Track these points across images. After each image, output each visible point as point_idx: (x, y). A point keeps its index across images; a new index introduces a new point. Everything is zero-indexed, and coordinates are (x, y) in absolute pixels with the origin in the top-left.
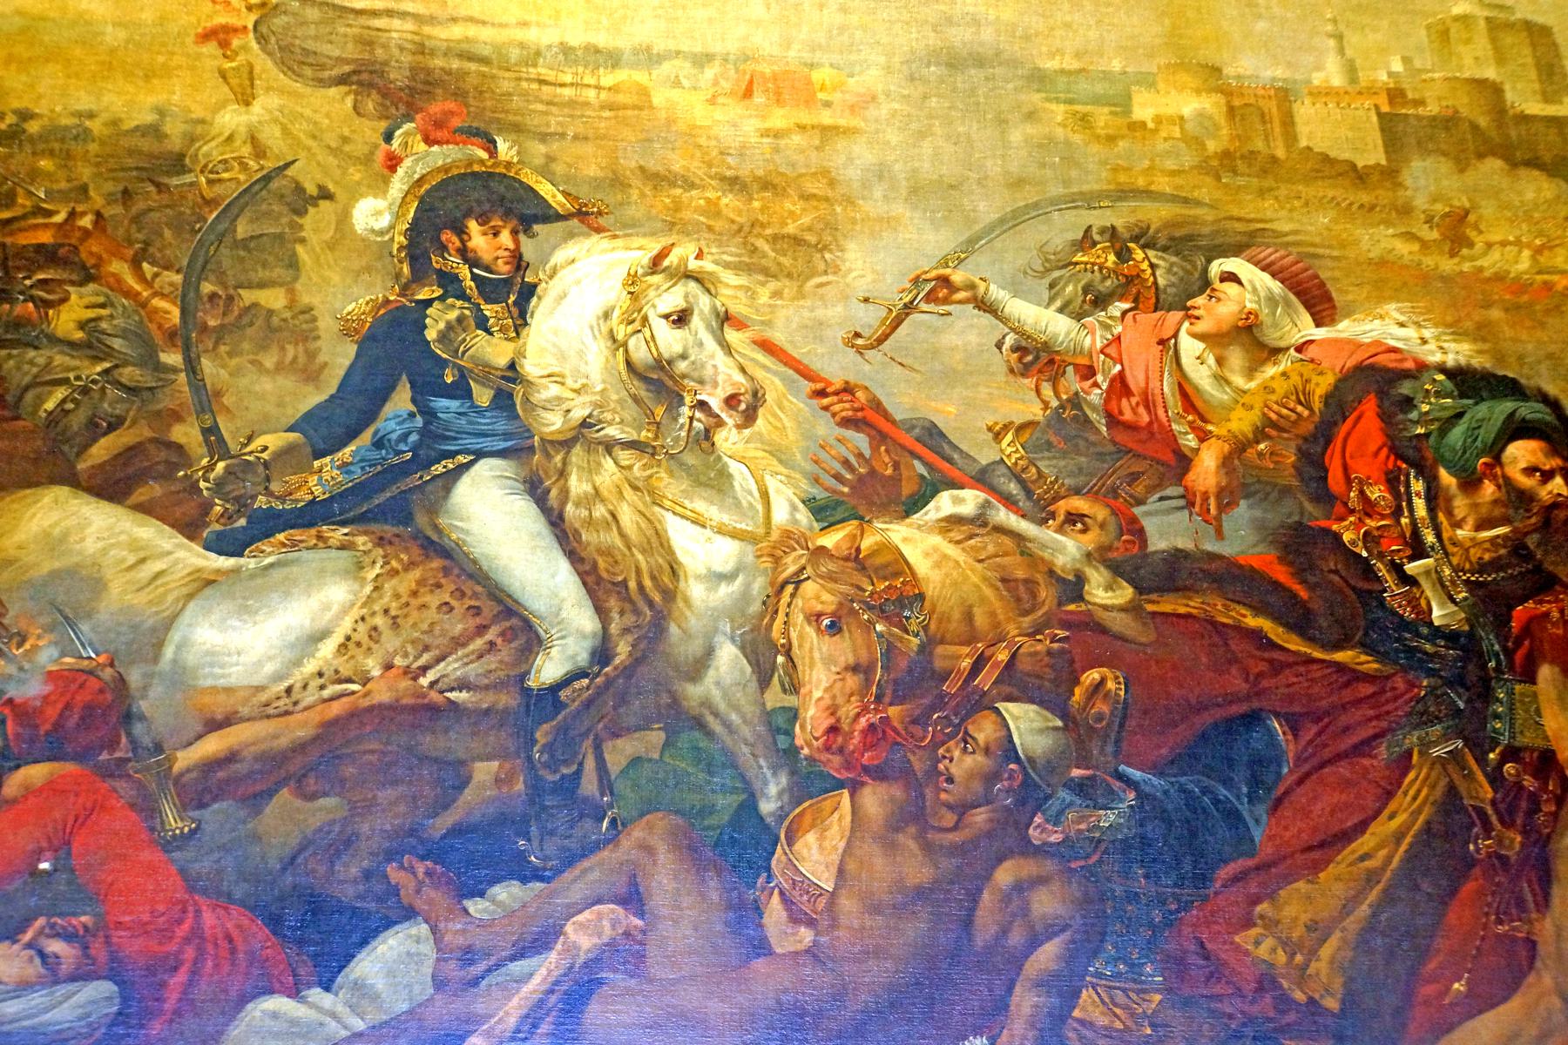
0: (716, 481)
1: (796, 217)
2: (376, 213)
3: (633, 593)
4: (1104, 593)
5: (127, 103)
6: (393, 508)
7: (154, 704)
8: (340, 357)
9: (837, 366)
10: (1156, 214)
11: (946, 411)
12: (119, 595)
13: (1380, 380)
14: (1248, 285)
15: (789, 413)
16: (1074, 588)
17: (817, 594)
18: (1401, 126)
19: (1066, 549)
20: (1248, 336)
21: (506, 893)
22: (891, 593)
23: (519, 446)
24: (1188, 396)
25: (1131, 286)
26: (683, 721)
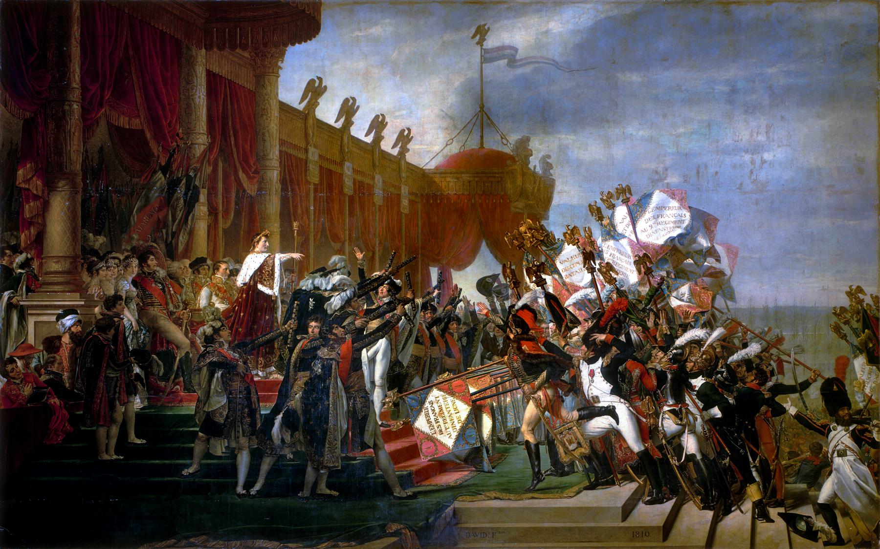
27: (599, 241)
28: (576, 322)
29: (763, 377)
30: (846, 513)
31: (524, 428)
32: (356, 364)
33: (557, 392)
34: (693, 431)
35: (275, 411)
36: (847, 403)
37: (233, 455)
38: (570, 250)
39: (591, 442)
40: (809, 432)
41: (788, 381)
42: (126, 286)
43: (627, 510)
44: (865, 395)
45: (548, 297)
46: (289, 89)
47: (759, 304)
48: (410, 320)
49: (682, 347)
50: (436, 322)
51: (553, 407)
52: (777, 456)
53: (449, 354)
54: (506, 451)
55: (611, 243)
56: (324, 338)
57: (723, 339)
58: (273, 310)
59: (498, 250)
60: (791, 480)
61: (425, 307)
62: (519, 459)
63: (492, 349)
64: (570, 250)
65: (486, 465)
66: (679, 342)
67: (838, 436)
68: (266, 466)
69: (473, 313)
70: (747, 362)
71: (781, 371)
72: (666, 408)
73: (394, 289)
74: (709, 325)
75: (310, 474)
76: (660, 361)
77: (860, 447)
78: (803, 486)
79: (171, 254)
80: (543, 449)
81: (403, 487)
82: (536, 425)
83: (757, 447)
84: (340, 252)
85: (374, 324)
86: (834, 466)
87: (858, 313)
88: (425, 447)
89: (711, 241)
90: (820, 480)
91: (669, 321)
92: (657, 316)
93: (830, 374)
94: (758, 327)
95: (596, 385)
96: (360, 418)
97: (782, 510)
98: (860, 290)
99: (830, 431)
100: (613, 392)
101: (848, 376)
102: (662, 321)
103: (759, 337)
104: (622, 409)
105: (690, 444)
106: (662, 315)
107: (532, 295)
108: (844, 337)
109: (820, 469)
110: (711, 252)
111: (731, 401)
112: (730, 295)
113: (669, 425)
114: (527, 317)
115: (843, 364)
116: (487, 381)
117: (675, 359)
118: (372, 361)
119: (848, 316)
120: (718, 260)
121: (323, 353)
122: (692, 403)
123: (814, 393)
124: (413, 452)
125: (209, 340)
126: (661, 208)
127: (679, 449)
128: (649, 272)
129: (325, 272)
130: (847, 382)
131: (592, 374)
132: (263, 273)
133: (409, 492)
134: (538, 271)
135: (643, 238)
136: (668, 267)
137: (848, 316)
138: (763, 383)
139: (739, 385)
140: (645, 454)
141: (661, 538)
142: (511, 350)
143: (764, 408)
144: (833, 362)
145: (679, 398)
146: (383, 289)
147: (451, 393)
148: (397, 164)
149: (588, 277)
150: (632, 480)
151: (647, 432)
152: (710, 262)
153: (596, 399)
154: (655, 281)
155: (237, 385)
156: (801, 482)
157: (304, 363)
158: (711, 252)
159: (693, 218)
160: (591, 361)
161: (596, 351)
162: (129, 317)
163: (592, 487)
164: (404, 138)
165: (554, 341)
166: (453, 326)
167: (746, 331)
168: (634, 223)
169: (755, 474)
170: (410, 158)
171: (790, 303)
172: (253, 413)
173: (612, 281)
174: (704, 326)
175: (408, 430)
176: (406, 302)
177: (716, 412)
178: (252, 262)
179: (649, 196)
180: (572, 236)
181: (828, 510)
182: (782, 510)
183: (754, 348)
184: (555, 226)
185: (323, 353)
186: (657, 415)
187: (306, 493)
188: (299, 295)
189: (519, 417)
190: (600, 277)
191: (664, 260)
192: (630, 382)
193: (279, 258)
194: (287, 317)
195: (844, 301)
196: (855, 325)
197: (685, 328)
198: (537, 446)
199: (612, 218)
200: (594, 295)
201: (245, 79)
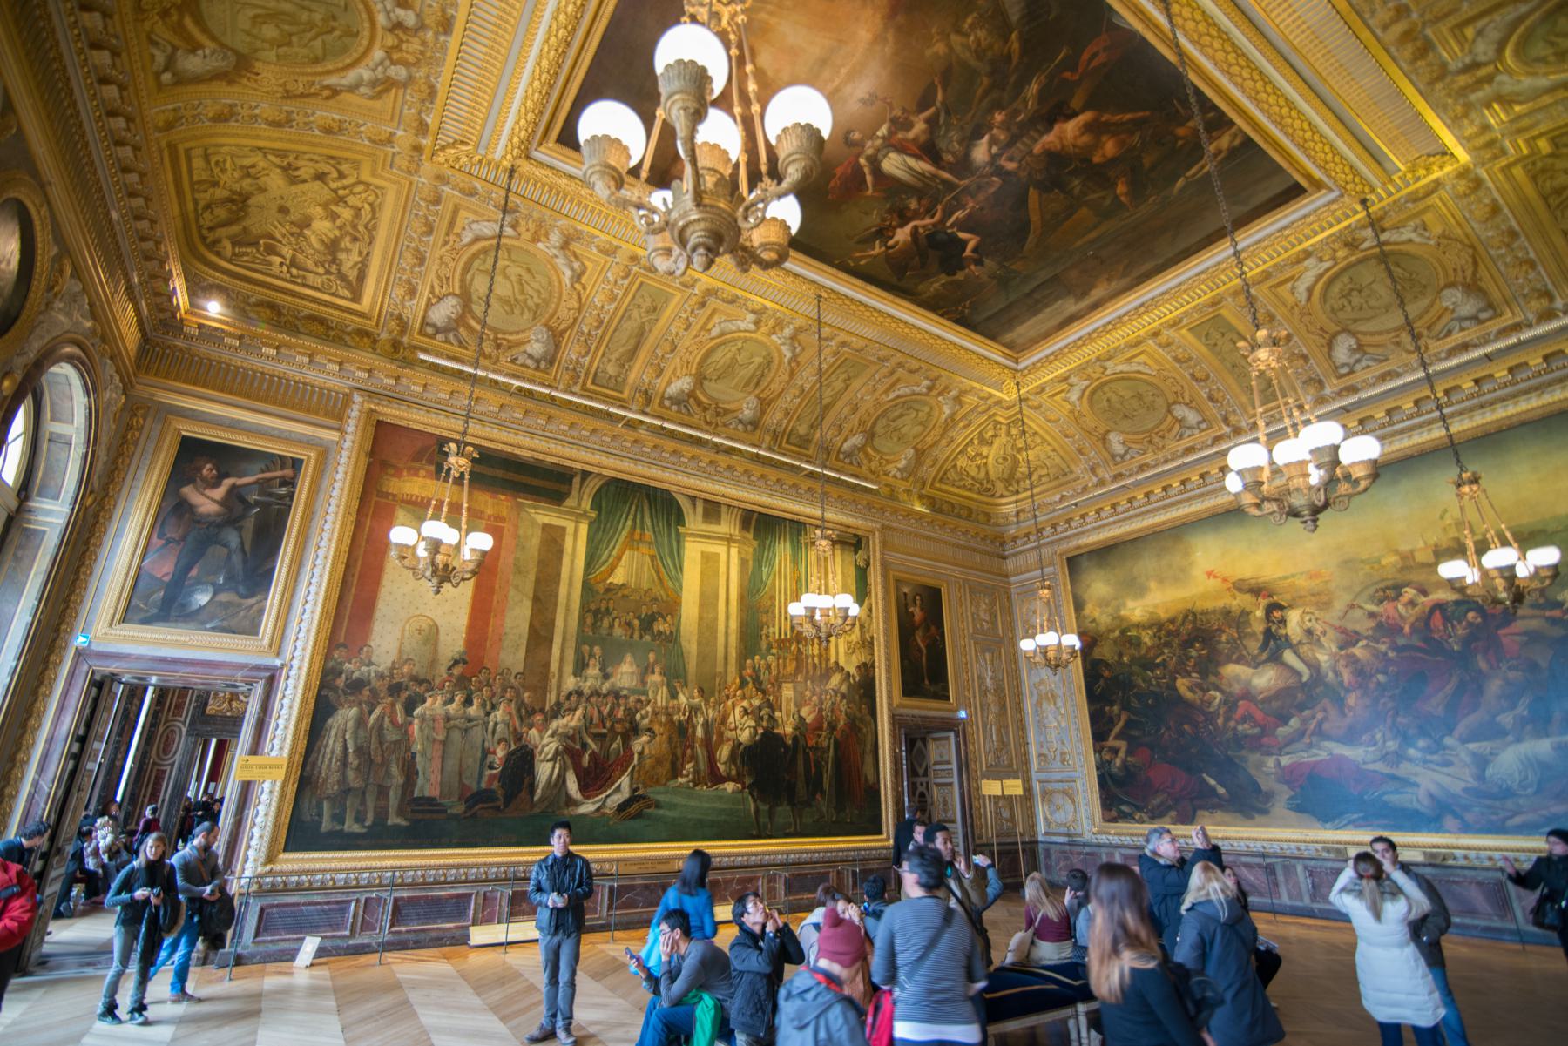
0: (1321, 646)
1: (1325, 598)
2: (1260, 613)
3: (1314, 666)
4: (1391, 654)
5: (1220, 604)
6: (1275, 658)
8: (1261, 637)
9: (1337, 623)
10: (1389, 583)
11: (1358, 627)
13: (1439, 606)
14: (1409, 593)
15: (1331, 633)
16: (1385, 654)
17: (1342, 662)
20: (1412, 603)
21: (1307, 713)
22: (1353, 660)
23: (1290, 646)
24: (1401, 616)
25: (1387, 598)
26: (1326, 685)
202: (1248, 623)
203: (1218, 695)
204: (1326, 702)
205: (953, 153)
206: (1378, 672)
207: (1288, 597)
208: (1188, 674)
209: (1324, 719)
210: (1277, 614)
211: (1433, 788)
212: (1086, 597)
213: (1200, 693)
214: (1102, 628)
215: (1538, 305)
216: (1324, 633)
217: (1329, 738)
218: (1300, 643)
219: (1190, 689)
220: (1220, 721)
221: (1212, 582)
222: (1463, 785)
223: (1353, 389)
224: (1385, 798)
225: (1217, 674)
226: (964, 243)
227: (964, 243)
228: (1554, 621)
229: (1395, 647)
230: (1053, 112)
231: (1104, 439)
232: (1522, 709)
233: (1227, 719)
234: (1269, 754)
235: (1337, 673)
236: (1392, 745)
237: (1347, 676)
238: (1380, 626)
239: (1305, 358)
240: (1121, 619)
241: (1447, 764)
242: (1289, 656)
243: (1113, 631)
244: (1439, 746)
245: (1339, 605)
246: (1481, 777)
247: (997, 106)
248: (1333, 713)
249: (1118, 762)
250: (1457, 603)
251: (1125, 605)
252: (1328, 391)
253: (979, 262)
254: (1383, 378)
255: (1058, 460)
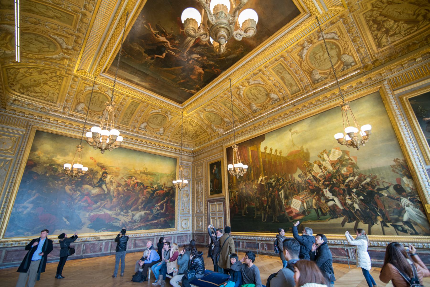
0: (112, 185)
1: (118, 174)
2: (101, 173)
3: (109, 190)
4: (126, 191)
6: (100, 186)
7: (90, 194)
8: (99, 180)
9: (118, 181)
11: (122, 183)
12: (89, 189)
13: (137, 183)
14: (134, 178)
15: (116, 183)
18: (141, 172)
19: (125, 189)
20: (133, 181)
21: (103, 201)
22: (118, 190)
25: (129, 178)
26: (110, 195)
27: (322, 162)
28: (320, 180)
29: (373, 187)
30: (416, 224)
31: (313, 205)
32: (279, 195)
33: (319, 197)
34: (356, 203)
35: (267, 206)
36: (404, 191)
37: (261, 215)
38: (316, 166)
39: (330, 207)
40: (393, 200)
41: (382, 187)
42: (244, 186)
43: (343, 224)
44: (410, 188)
45: (313, 176)
46: (262, 149)
47: (367, 168)
48: (287, 185)
49: (348, 182)
50: (291, 185)
51: (319, 200)
52: (384, 208)
53: (295, 191)
54: (310, 211)
55: (324, 162)
56: (273, 191)
57: (358, 179)
58: (264, 187)
59: (301, 168)
60: (391, 215)
61: (289, 182)
62: (313, 213)
63: (303, 189)
64: (316, 166)
65: (307, 214)
66: (346, 181)
67: (405, 201)
68: (266, 216)
69: (298, 182)
70: (367, 184)
71: (379, 184)
72: (347, 198)
73: (283, 180)
74: (354, 176)
75: (274, 218)
76: (343, 186)
77: (414, 203)
78: (396, 216)
79: (249, 180)
80: (319, 210)
81: (291, 220)
82: (316, 204)
83: (377, 206)
84: (273, 175)
85: (281, 187)
86: (406, 210)
87: (399, 165)
88: (294, 211)
89: (349, 156)
90: (402, 214)
91: (343, 177)
92: (339, 176)
93: (395, 183)
94: (368, 174)
95: (328, 195)
96: (281, 205)
97: (391, 224)
98: (397, 159)
99: (401, 199)
100: (332, 195)
101: (402, 183)
102: (341, 177)
103: (369, 177)
104: (336, 199)
105: (356, 206)
106: (340, 176)
107: (309, 176)
108: (397, 173)
109: (401, 211)
110: (349, 159)
111: (365, 194)
112: (358, 168)
113: (349, 202)
114: (309, 181)
115: (399, 180)
116: (303, 196)
117: (346, 186)
118: (281, 194)
119: (396, 167)
120: (352, 160)
121: (273, 194)
122: (354, 195)
123: (391, 189)
124: (291, 212)
125: (255, 193)
126: (334, 152)
127: (354, 208)
128: (335, 167)
129: (271, 179)
130: (402, 185)
131: (326, 191)
132: (262, 181)
133: (292, 221)
134: (310, 171)
135: (331, 159)
136: (339, 164)
137: (396, 167)
138: (374, 188)
139: (367, 190)
140: (344, 210)
141: (354, 231)
142: (307, 189)
143: (376, 195)
144: (395, 180)
145: (350, 195)
146: (281, 180)
147: (297, 199)
148: (280, 157)
149: (321, 170)
150: (342, 216)
151: (344, 204)
152: (350, 161)
153: (329, 197)
154: (337, 168)
155: (260, 201)
156: (395, 215)
157: (270, 196)
158: (349, 159)
159: (343, 152)
160: (325, 189)
161: (326, 186)
162: (244, 191)
163: (332, 218)
164: (281, 152)
165: (316, 185)
166: (295, 185)
167: (364, 176)
168: (328, 157)
169: (378, 213)
170: (282, 155)
171: (376, 167)
172: (263, 206)
173: (326, 170)
174: (352, 176)
175: (290, 207)
176: (285, 182)
177: (361, 197)
178: (260, 179)
179: (331, 150)
180: (315, 162)
181: (408, 223)
182: (391, 224)
183: (368, 180)
184: (311, 161)
185: (273, 194)
186: (345, 200)
187: (273, 221)
188: (268, 183)
189: (312, 203)
190: (323, 170)
191: (337, 164)
192: (336, 193)
193: (264, 177)
194: (266, 188)
195: (394, 163)
196: (399, 169)
197: (347, 178)
198: (317, 209)
199: (323, 157)
200: (323, 174)
201: (256, 150)
202: (97, 175)
203: (79, 193)
204: (108, 200)
205: (195, 50)
206: (122, 194)
207: (110, 171)
208: (72, 185)
209: (107, 204)
210: (105, 175)
211: (123, 221)
212: (39, 147)
213: (73, 191)
214: (42, 161)
215: (167, 138)
216: (114, 183)
217: (106, 208)
218: (108, 183)
219: (70, 190)
220: (76, 201)
221: (91, 160)
222: (129, 220)
223: (138, 133)
224: (113, 224)
225: (81, 187)
226: (161, 55)
227: (161, 55)
228: (152, 190)
229: (127, 190)
230: (204, 67)
231: (78, 103)
232: (142, 206)
233: (79, 200)
234: (88, 212)
235: (113, 193)
236: (119, 211)
237: (115, 194)
238: (126, 184)
239: (138, 122)
240: (52, 161)
241: (128, 216)
242: (104, 186)
243: (46, 163)
244: (127, 212)
245: (120, 177)
246: (132, 219)
247: (208, 57)
248: (109, 202)
249: (25, 212)
250: (140, 183)
251: (56, 156)
252: (135, 130)
253: (152, 59)
254: (144, 134)
255: (55, 97)
